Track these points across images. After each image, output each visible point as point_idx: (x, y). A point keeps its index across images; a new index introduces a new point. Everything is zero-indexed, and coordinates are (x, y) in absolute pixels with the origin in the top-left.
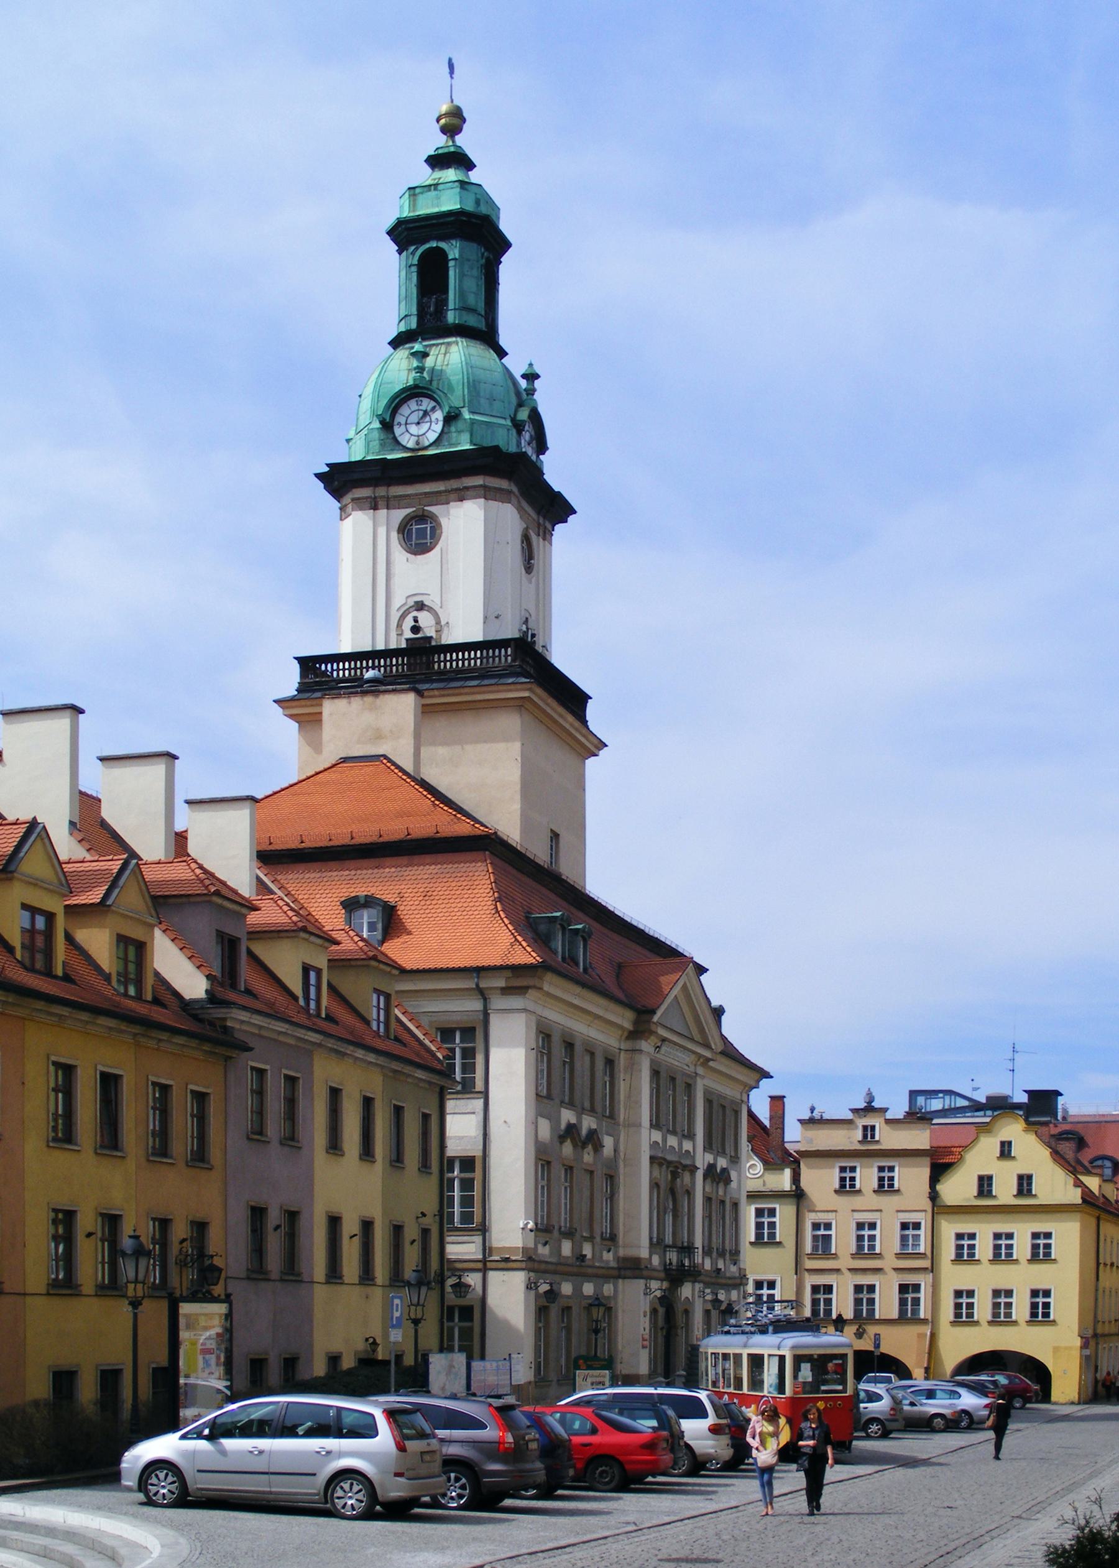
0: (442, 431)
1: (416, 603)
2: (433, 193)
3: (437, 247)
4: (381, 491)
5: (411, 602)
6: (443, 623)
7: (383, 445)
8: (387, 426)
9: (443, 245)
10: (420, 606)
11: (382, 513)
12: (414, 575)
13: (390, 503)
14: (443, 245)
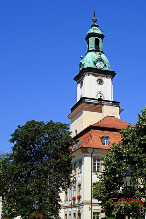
0: (104, 67)
1: (100, 93)
2: (97, 30)
3: (98, 39)
4: (94, 73)
5: (99, 92)
6: (104, 97)
7: (94, 66)
8: (95, 63)
9: (99, 38)
10: (100, 93)
11: (94, 77)
12: (99, 88)
13: (96, 76)
14: (99, 38)
